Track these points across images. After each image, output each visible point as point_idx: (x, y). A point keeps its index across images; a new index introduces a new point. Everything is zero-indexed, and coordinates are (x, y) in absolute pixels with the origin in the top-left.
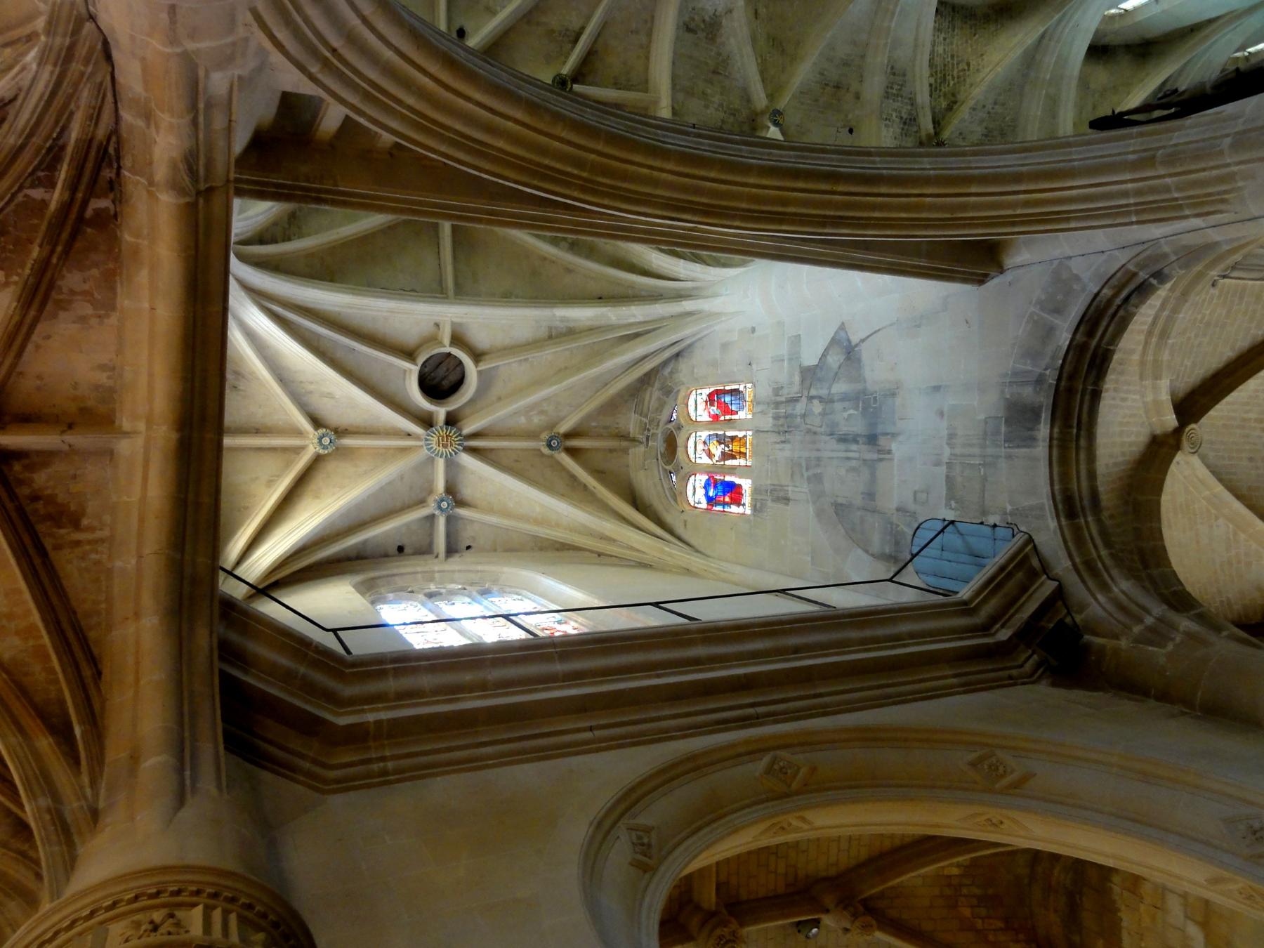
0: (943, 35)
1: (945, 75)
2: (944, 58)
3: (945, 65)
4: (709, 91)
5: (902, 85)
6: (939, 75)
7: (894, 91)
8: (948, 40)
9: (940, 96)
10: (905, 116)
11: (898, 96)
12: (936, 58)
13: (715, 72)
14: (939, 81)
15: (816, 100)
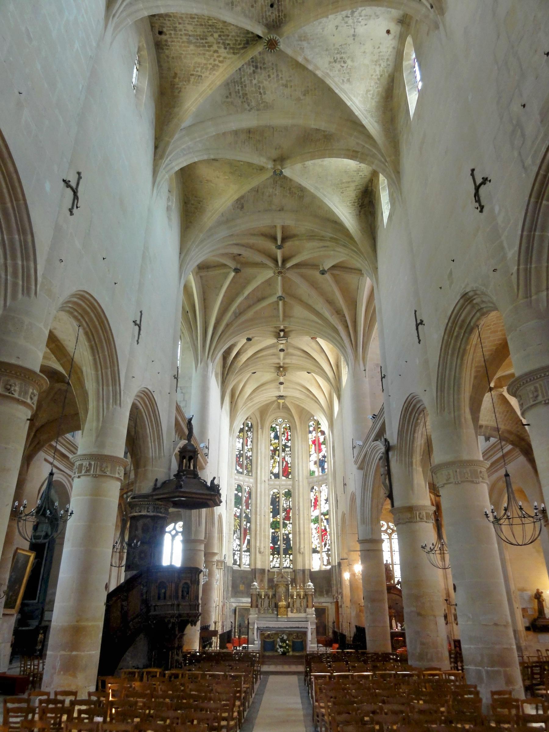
0: (177, 25)
1: (210, 26)
2: (196, 25)
3: (201, 25)
4: (267, 194)
5: (234, 82)
6: (210, 29)
7: (240, 88)
8: (180, 21)
9: (227, 29)
10: (252, 69)
11: (241, 83)
12: (198, 33)
13: (257, 191)
14: (215, 30)
15: (259, 141)
